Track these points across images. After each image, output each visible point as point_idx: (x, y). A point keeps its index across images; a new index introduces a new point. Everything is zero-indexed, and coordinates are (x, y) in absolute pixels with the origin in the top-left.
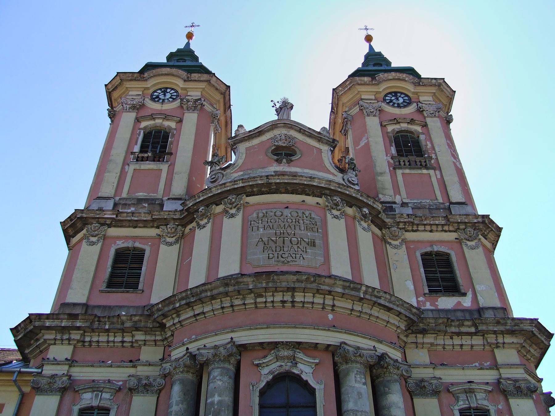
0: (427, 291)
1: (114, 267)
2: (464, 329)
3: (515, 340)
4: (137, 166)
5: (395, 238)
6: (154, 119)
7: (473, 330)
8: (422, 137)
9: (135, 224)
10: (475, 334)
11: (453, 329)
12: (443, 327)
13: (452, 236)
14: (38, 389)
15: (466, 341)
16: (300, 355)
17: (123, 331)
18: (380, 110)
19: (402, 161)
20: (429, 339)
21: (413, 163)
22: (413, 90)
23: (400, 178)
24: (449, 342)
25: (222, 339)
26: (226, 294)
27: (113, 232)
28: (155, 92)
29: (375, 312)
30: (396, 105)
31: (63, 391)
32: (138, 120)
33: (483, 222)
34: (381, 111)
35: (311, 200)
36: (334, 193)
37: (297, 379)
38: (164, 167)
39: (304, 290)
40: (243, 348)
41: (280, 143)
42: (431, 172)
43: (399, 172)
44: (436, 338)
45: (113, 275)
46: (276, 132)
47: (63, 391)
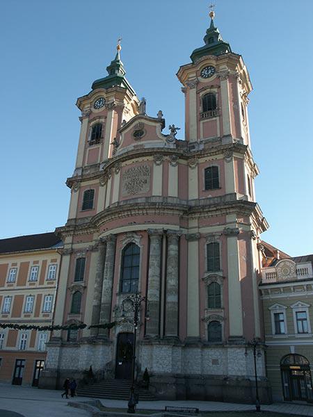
0: (204, 189)
1: (84, 200)
2: (211, 209)
3: (234, 210)
4: (90, 148)
5: (193, 163)
7: (215, 209)
8: (217, 95)
9: (89, 179)
10: (217, 210)
11: (207, 210)
12: (201, 210)
13: (220, 157)
14: (64, 254)
15: (214, 213)
16: (135, 236)
17: (86, 229)
20: (198, 215)
21: (209, 115)
23: (201, 125)
24: (206, 215)
25: (108, 233)
26: (108, 215)
27: (83, 184)
29: (166, 211)
31: (71, 254)
32: (89, 122)
33: (234, 147)
34: (198, 83)
35: (145, 158)
36: (156, 153)
37: (134, 244)
38: (100, 146)
39: (134, 209)
40: (116, 235)
41: (137, 129)
42: (218, 118)
43: (202, 122)
45: (84, 204)
46: (136, 122)
47: (71, 254)
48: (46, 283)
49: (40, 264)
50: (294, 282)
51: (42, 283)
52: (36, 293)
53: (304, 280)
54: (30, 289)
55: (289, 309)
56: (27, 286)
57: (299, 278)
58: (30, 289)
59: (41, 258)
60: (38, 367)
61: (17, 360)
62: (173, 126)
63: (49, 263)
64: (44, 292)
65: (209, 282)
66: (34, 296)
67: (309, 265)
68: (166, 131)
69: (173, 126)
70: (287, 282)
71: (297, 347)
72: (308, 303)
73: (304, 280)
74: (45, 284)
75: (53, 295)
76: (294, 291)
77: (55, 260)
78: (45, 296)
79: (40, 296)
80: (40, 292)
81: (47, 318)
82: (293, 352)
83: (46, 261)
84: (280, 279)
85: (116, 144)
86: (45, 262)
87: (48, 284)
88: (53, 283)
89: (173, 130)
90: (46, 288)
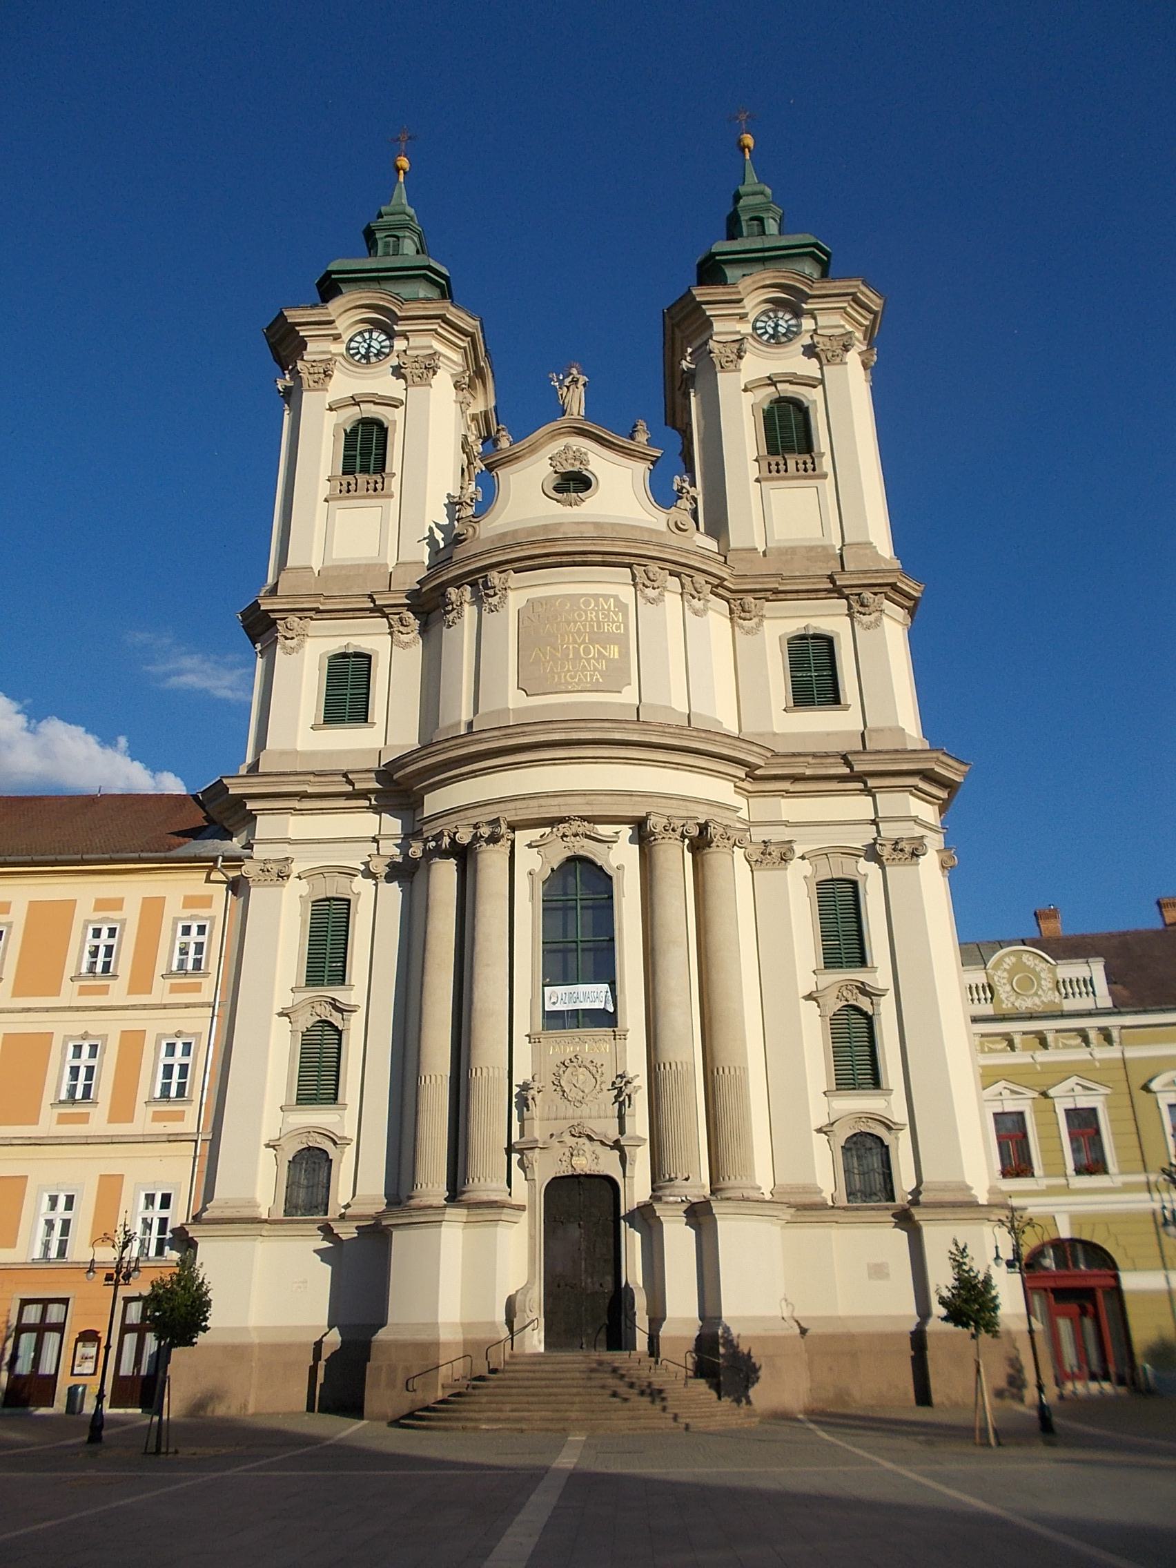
19: (773, 463)
28: (351, 340)
49: (131, 914)
51: (141, 982)
52: (111, 1028)
53: (1089, 1014)
54: (78, 1009)
56: (69, 994)
57: (1069, 1005)
58: (78, 1009)
60: (29, 1328)
61: (25, 1302)
63: (174, 910)
64: (156, 1026)
66: (104, 1037)
67: (1096, 970)
70: (1031, 1017)
71: (1075, 1220)
73: (1089, 1014)
74: (161, 991)
75: (198, 1035)
76: (1057, 1047)
78: (160, 1037)
79: (132, 1042)
80: (133, 1020)
81: (174, 1127)
82: (1065, 1233)
84: (1006, 1006)
86: (153, 908)
87: (174, 989)
90: (165, 1007)
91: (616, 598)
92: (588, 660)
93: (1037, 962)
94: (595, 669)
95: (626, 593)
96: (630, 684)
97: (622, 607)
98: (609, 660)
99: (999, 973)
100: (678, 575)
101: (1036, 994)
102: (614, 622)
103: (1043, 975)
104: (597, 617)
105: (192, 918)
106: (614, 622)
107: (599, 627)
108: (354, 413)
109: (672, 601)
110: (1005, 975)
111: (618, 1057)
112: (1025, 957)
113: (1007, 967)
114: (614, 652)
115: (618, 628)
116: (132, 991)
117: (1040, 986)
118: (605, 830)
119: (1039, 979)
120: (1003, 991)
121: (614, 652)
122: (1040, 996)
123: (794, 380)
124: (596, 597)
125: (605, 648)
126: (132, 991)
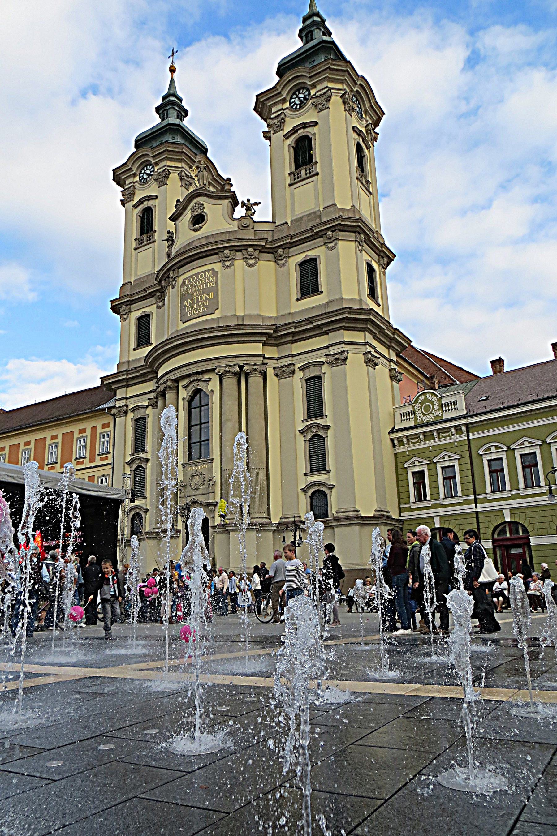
6: (142, 203)
7: (310, 326)
18: (283, 122)
22: (309, 83)
30: (298, 107)
44: (293, 337)
48: (98, 458)
49: (88, 433)
50: (436, 423)
53: (452, 419)
55: (432, 464)
59: (88, 425)
62: (249, 200)
63: (99, 430)
65: (310, 435)
68: (240, 212)
69: (249, 200)
72: (425, 459)
73: (452, 419)
75: (108, 475)
76: (439, 438)
77: (108, 425)
78: (99, 477)
80: (90, 473)
83: (96, 427)
85: (171, 240)
87: (101, 459)
88: (106, 458)
89: (249, 207)
91: (213, 270)
92: (201, 302)
93: (433, 397)
94: (204, 305)
95: (217, 267)
96: (218, 309)
97: (216, 274)
98: (209, 300)
99: (417, 405)
100: (240, 251)
101: (431, 413)
102: (212, 281)
103: (435, 403)
104: (205, 281)
105: (105, 432)
106: (212, 281)
107: (206, 286)
108: (141, 207)
109: (239, 264)
110: (420, 405)
111: (211, 470)
112: (428, 395)
113: (420, 401)
114: (212, 295)
115: (213, 284)
116: (91, 462)
117: (433, 408)
118: (206, 376)
119: (433, 405)
120: (418, 413)
121: (212, 295)
122: (433, 414)
123: (305, 126)
124: (204, 272)
125: (208, 295)
126: (90, 462)
